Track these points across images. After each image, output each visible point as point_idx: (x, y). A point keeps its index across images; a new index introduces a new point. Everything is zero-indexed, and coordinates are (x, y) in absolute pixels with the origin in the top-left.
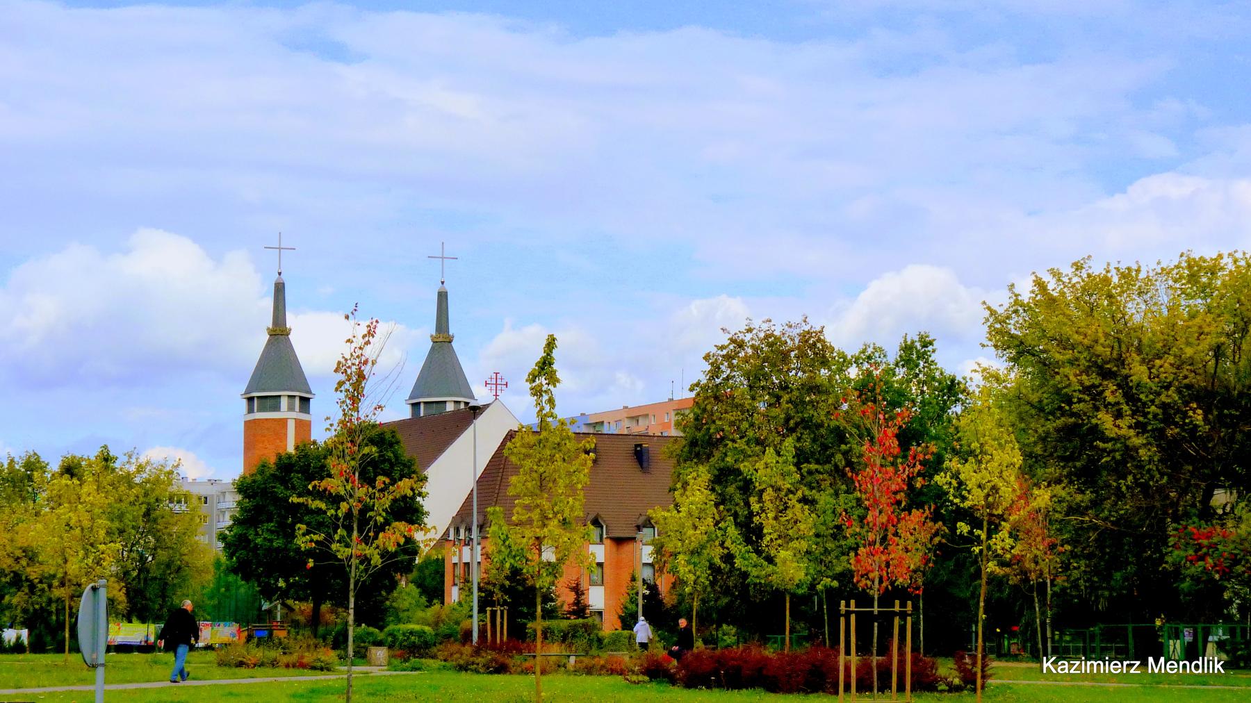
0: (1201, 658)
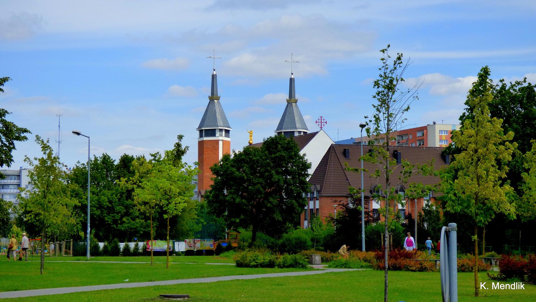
0: (515, 283)
